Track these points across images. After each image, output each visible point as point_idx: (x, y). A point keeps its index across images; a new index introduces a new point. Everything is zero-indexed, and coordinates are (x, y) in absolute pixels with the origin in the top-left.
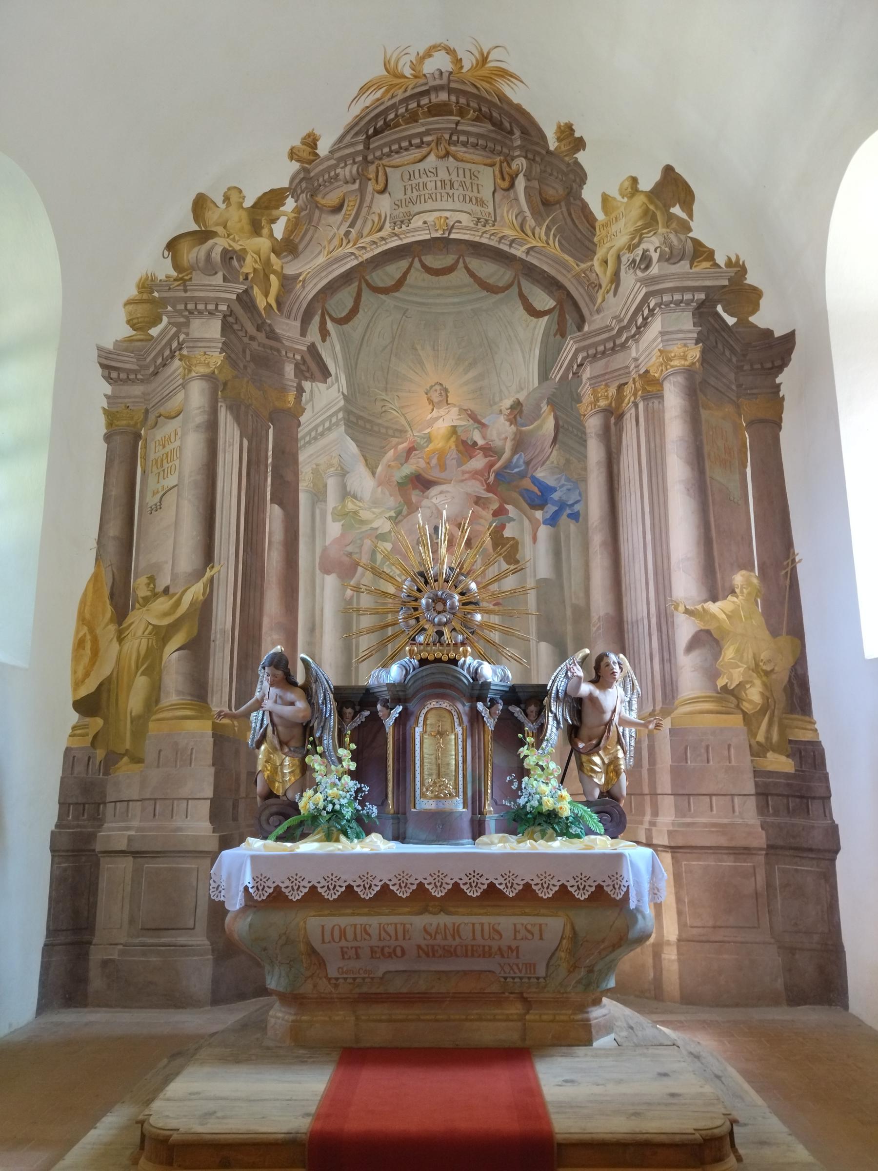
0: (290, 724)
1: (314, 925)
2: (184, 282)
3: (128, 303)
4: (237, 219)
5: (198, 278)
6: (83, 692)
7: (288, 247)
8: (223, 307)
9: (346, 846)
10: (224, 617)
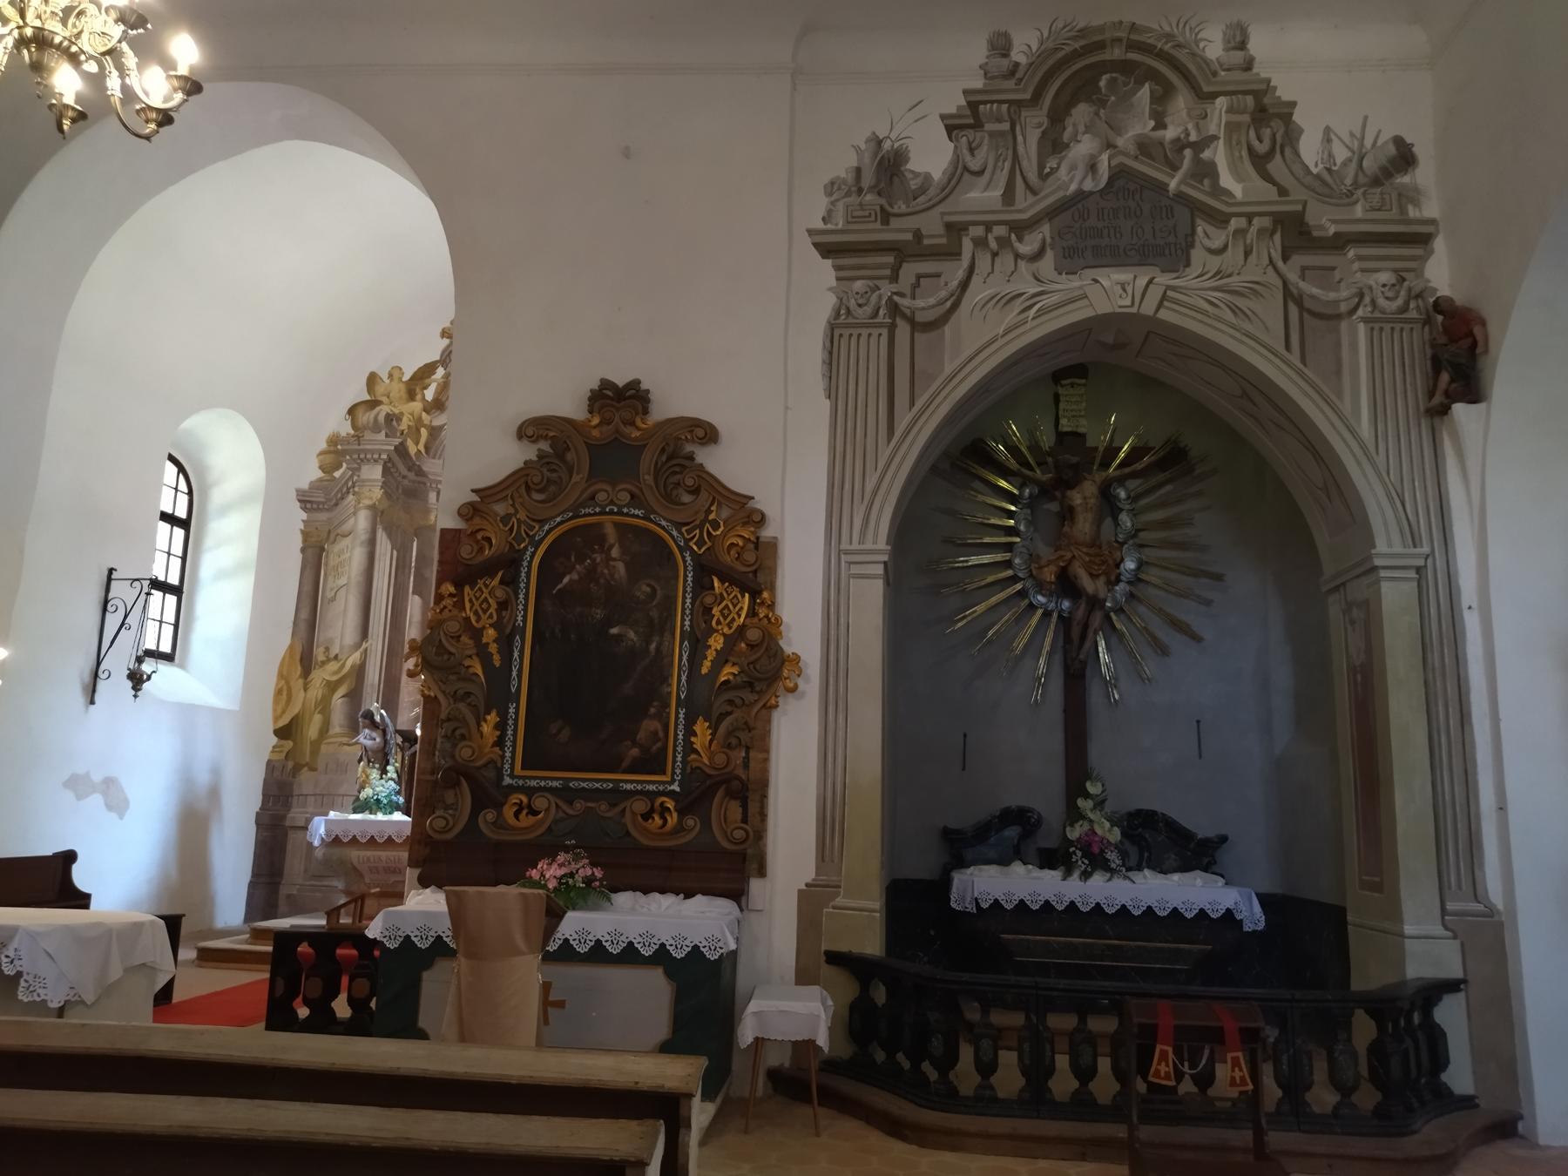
0: (375, 752)
1: (355, 855)
2: (358, 438)
3: (321, 454)
4: (398, 390)
5: (368, 435)
6: (281, 723)
8: (384, 456)
9: (380, 817)
10: (374, 675)
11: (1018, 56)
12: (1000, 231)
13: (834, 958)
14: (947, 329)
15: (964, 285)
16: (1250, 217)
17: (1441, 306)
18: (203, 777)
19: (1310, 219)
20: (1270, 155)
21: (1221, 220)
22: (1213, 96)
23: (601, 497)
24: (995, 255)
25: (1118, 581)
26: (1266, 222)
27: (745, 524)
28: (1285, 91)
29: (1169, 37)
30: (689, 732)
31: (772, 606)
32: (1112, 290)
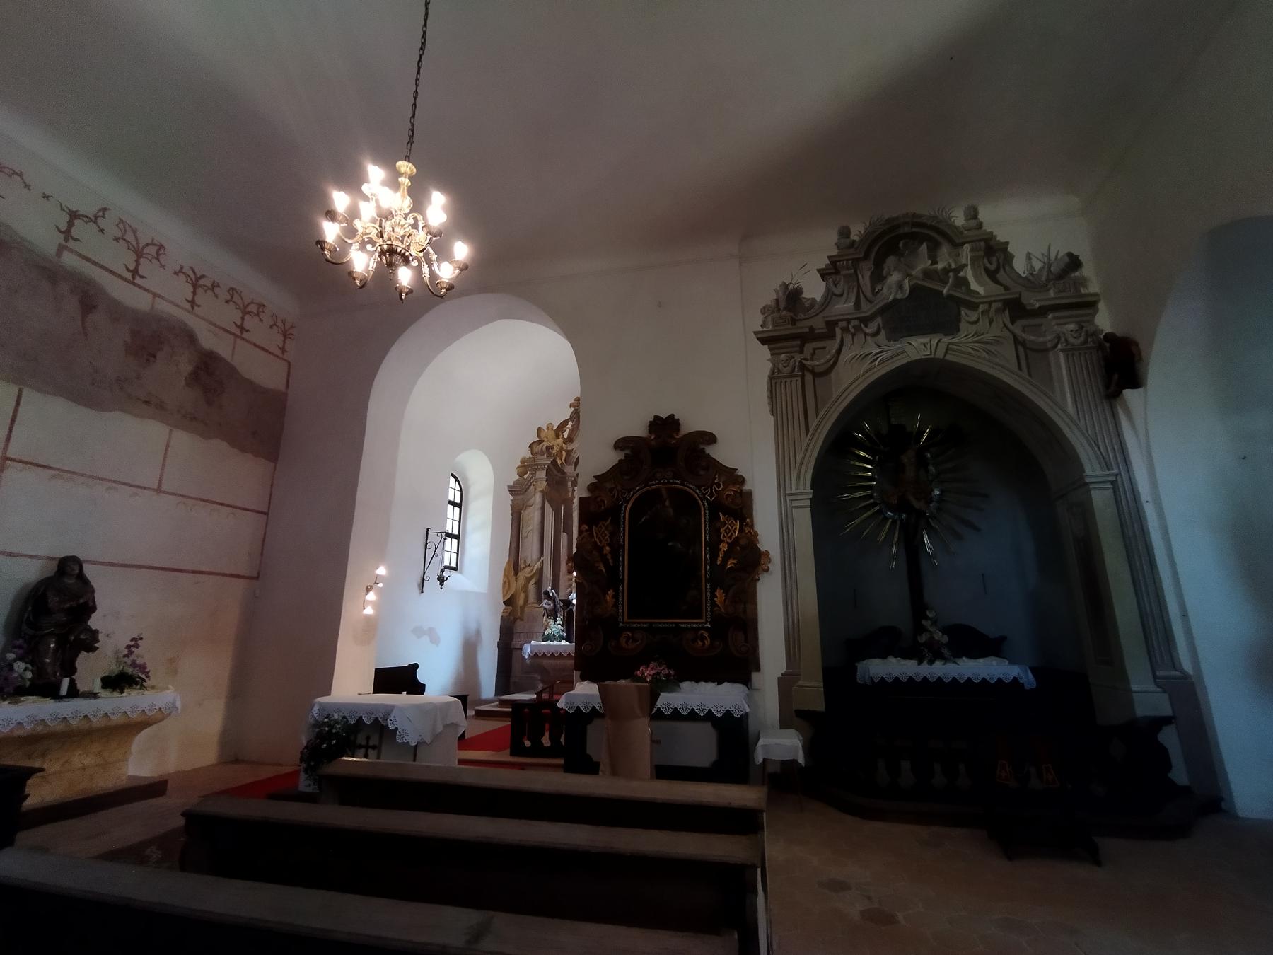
1: (545, 662)
4: (552, 434)
5: (539, 457)
7: (570, 440)
9: (555, 643)
11: (854, 237)
12: (855, 323)
13: (801, 714)
14: (833, 375)
15: (839, 352)
16: (990, 303)
17: (1109, 337)
18: (473, 626)
19: (1024, 301)
20: (997, 270)
21: (973, 306)
22: (962, 244)
23: (658, 475)
24: (853, 335)
25: (931, 502)
26: (999, 305)
27: (734, 484)
28: (1002, 238)
29: (935, 217)
30: (713, 596)
31: (752, 526)
32: (919, 347)
